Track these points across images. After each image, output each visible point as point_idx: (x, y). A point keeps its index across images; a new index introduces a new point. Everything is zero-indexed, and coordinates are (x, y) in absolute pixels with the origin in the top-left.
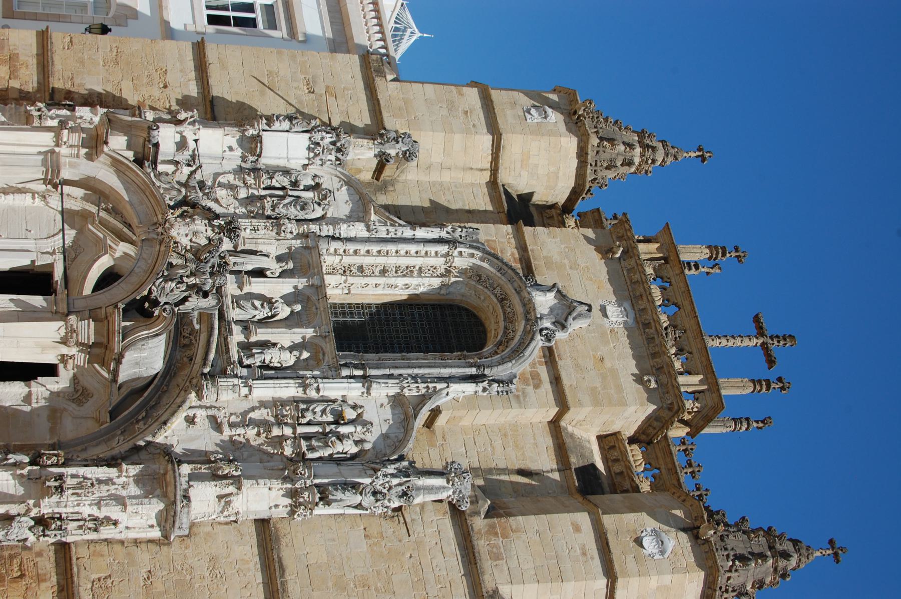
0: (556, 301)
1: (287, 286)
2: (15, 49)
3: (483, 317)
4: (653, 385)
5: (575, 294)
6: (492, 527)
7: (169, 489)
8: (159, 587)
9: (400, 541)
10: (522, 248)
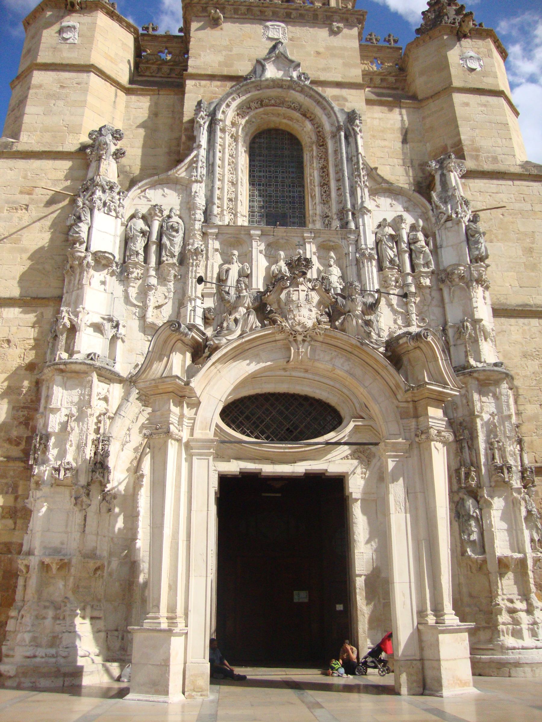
3: (265, 127)
4: (341, 25)
5: (263, 53)
6: (472, 157)
7: (492, 378)
9: (491, 219)
10: (212, 77)
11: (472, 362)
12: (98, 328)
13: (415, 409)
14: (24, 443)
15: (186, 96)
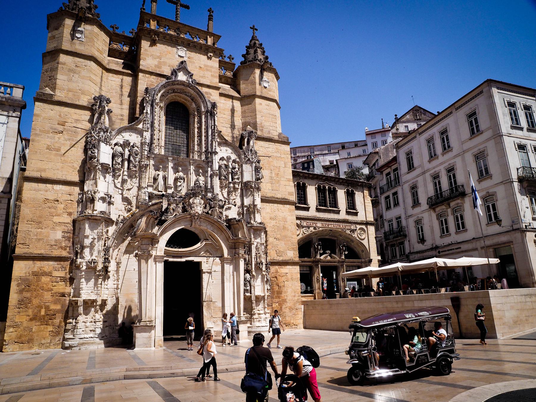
0: (182, 72)
1: (171, 171)
2: (29, 273)
4: (212, 54)
8: (279, 236)
10: (151, 73)
11: (252, 222)
12: (103, 199)
13: (235, 245)
14: (68, 249)
15: (139, 81)
